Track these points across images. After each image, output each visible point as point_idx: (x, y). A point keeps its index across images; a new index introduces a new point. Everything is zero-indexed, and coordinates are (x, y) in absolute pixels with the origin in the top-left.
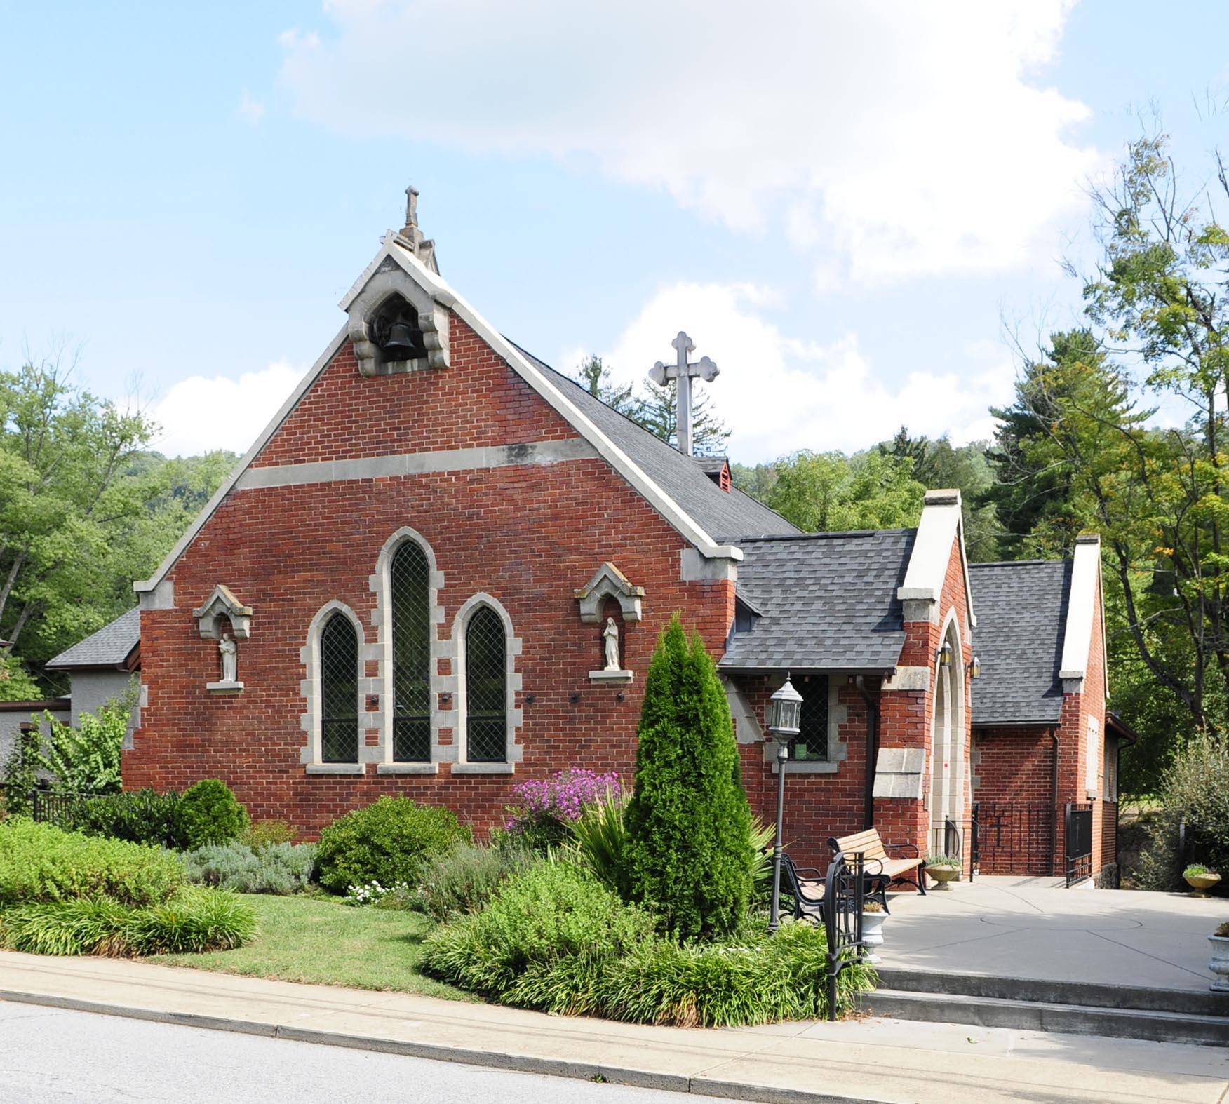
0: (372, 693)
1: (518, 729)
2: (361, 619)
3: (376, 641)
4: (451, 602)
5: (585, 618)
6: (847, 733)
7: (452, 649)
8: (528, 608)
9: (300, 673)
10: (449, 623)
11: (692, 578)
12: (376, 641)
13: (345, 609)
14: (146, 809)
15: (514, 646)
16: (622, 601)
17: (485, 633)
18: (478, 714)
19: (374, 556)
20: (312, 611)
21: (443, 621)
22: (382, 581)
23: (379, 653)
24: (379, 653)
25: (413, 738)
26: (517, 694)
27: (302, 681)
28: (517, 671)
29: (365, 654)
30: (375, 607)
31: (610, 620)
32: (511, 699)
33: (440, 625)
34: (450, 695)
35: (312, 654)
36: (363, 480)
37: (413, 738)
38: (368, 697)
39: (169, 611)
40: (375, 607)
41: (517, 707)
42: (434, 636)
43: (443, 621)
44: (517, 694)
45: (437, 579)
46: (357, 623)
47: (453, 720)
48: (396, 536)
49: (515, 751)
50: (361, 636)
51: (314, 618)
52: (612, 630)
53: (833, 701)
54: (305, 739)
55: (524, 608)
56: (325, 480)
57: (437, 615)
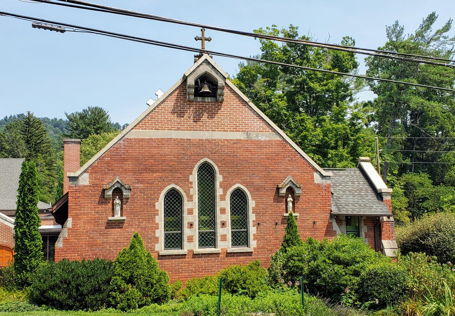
0: (190, 221)
1: (254, 235)
2: (185, 192)
3: (192, 201)
4: (225, 188)
5: (280, 195)
6: (367, 235)
7: (223, 204)
8: (257, 190)
9: (156, 213)
10: (225, 194)
11: (318, 182)
12: (192, 201)
13: (178, 188)
14: (440, 157)
15: (252, 204)
16: (296, 189)
17: (239, 200)
18: (234, 230)
19: (192, 168)
20: (162, 189)
21: (222, 193)
22: (194, 177)
23: (191, 206)
24: (191, 206)
25: (207, 239)
26: (253, 221)
27: (156, 217)
28: (253, 213)
29: (187, 205)
30: (192, 187)
31: (290, 195)
32: (251, 224)
33: (221, 196)
34: (225, 222)
35: (160, 205)
36: (187, 139)
37: (207, 239)
38: (188, 223)
39: (86, 186)
40: (192, 187)
41: (254, 226)
42: (218, 199)
43: (222, 193)
44: (253, 221)
45: (219, 178)
46: (184, 194)
47: (224, 232)
48: (202, 161)
49: (253, 243)
50: (185, 198)
51: (163, 192)
52: (290, 199)
53: (362, 224)
54: (158, 241)
55: (256, 190)
56: (169, 137)
57: (219, 192)
